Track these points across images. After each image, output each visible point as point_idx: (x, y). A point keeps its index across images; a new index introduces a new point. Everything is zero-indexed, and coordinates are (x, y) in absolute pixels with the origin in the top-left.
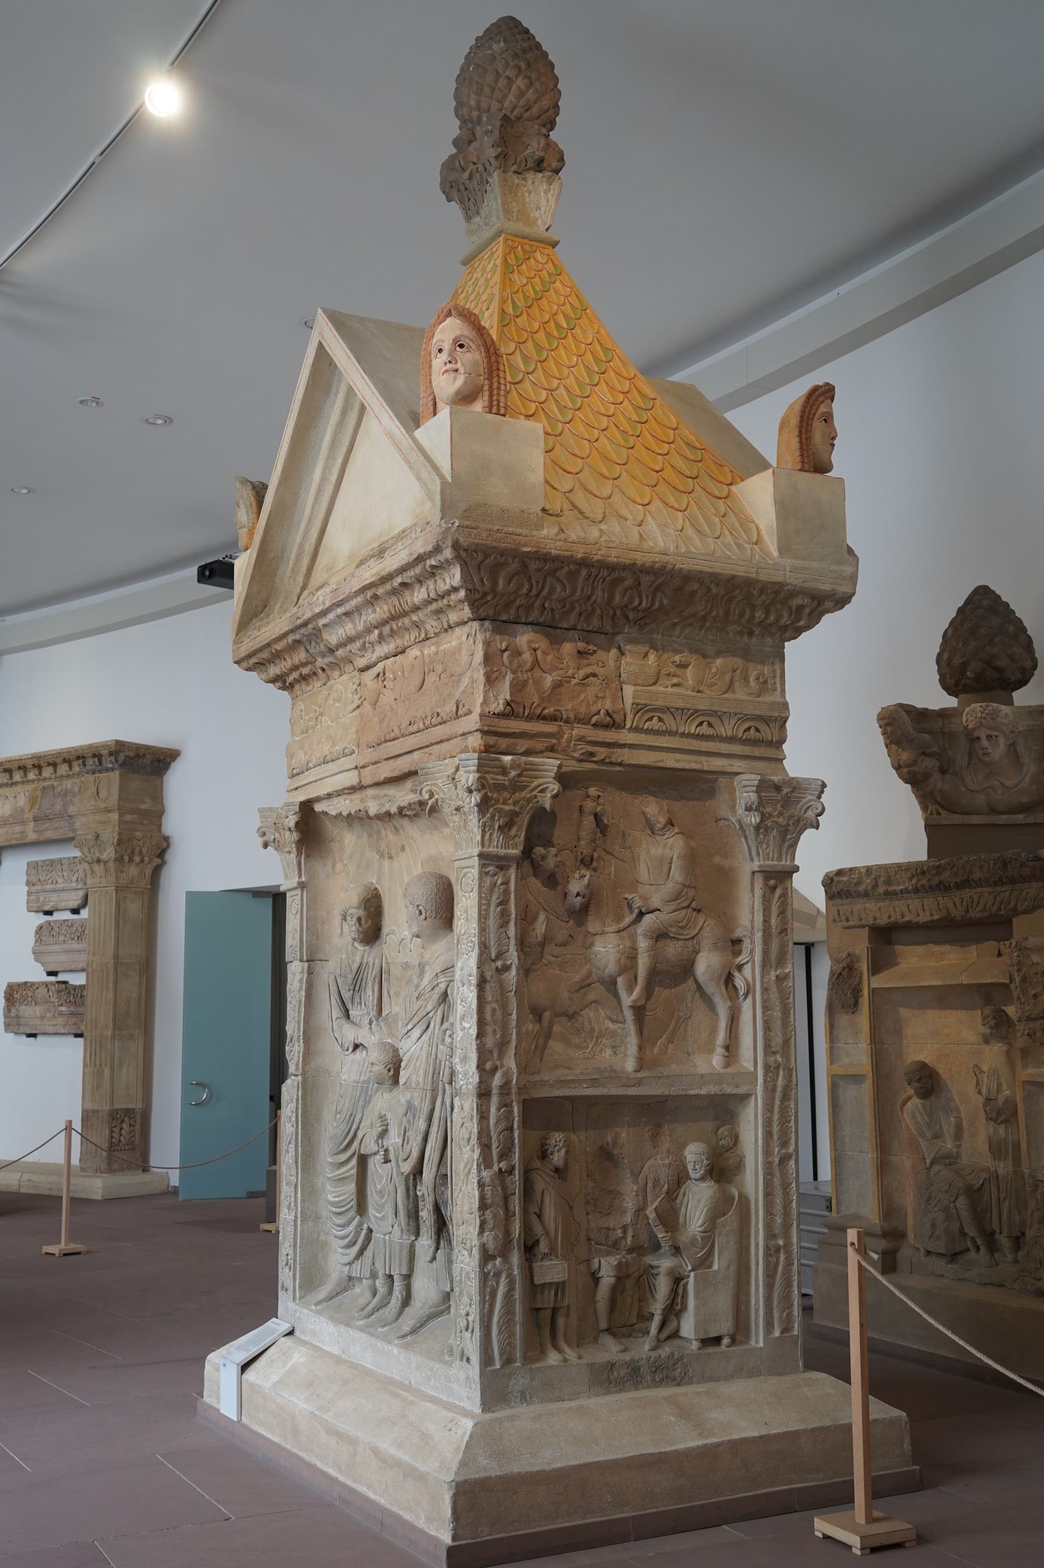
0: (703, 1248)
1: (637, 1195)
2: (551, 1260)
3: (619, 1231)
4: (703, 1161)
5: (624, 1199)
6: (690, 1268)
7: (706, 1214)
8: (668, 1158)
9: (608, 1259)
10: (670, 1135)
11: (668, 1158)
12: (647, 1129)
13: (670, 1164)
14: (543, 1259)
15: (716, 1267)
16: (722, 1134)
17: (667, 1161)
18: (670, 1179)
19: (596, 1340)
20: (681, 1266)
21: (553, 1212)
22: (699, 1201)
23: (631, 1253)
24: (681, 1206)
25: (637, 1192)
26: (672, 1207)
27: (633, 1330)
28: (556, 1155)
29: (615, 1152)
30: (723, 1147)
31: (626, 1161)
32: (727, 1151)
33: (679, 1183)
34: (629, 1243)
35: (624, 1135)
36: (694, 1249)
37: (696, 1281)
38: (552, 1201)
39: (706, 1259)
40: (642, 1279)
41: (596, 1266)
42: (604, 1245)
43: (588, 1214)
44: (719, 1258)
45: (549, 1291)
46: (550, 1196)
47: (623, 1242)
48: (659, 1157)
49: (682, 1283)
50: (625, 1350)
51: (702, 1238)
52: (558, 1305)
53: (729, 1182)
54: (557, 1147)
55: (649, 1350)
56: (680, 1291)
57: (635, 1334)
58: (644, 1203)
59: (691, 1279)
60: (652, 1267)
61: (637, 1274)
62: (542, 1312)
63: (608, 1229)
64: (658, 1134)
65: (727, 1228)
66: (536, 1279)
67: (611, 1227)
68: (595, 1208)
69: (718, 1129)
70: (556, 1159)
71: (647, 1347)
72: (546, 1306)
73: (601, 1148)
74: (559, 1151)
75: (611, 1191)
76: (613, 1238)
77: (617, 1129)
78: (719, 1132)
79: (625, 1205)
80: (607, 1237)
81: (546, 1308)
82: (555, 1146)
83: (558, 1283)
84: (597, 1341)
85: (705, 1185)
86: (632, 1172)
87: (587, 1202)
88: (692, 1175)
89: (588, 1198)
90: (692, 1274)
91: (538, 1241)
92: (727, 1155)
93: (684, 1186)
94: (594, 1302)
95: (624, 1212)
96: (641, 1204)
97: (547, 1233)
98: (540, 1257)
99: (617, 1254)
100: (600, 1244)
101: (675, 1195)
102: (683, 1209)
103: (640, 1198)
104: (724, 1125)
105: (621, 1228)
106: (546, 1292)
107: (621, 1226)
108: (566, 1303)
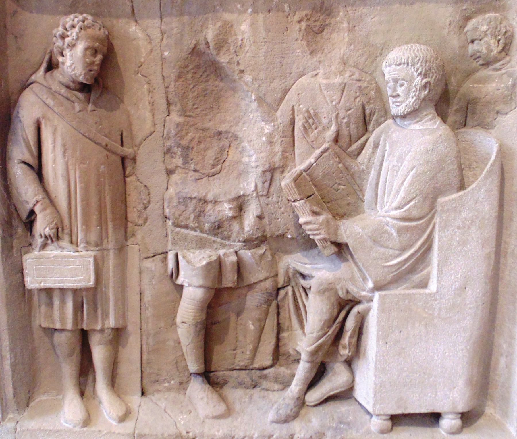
0: (403, 250)
1: (271, 143)
2: (63, 248)
3: (227, 206)
4: (412, 78)
5: (244, 150)
6: (370, 285)
7: (411, 184)
8: (342, 73)
9: (190, 256)
10: (351, 30)
11: (342, 73)
12: (297, 18)
13: (343, 87)
14: (44, 246)
15: (433, 287)
16: (476, 29)
17: (337, 80)
18: (342, 114)
19: (183, 385)
20: (352, 279)
21: (60, 161)
22: (401, 159)
23: (257, 246)
24: (369, 167)
25: (271, 135)
26: (347, 169)
27: (265, 377)
28: (67, 52)
29: (223, 59)
30: (475, 57)
31: (248, 78)
32: (487, 64)
33: (366, 123)
34: (247, 229)
35: (244, 27)
36: (382, 250)
37: (382, 309)
38: (59, 141)
39: (412, 270)
40: (282, 293)
41: (171, 264)
42: (194, 229)
43: (169, 172)
44: (440, 271)
45: (63, 302)
46: (54, 133)
47: (236, 226)
48: (321, 71)
49: (355, 310)
50: (229, 413)
51: (400, 231)
52: (85, 327)
53: (486, 126)
54: (67, 40)
55: (273, 422)
56: (350, 324)
57: (265, 384)
58: (284, 158)
59: (375, 305)
60: (303, 276)
61: (268, 284)
62: (57, 335)
63: (205, 201)
64: (321, 30)
65: (464, 215)
66: (28, 280)
67: (210, 197)
68: (186, 163)
69: (468, 19)
70: (68, 63)
71: (271, 416)
72: (58, 326)
73: (195, 51)
74: (72, 46)
75: (220, 133)
76: (212, 219)
77: (227, 16)
78: (471, 25)
79: (246, 159)
80: (200, 215)
81: (62, 330)
82: (63, 37)
83: (75, 291)
84: (185, 389)
85: (417, 127)
86: (260, 100)
87: (168, 151)
88: (396, 109)
89: (168, 143)
90: (377, 295)
91: (32, 213)
92: (484, 72)
93: (377, 130)
94: (174, 324)
95: (242, 174)
96: (277, 158)
97: (51, 202)
98: (39, 241)
99: (223, 246)
100: (186, 227)
101: (355, 146)
102: (373, 173)
103: (278, 148)
104: (480, 11)
105: (230, 201)
106: (57, 302)
107: (233, 195)
108: (111, 322)
